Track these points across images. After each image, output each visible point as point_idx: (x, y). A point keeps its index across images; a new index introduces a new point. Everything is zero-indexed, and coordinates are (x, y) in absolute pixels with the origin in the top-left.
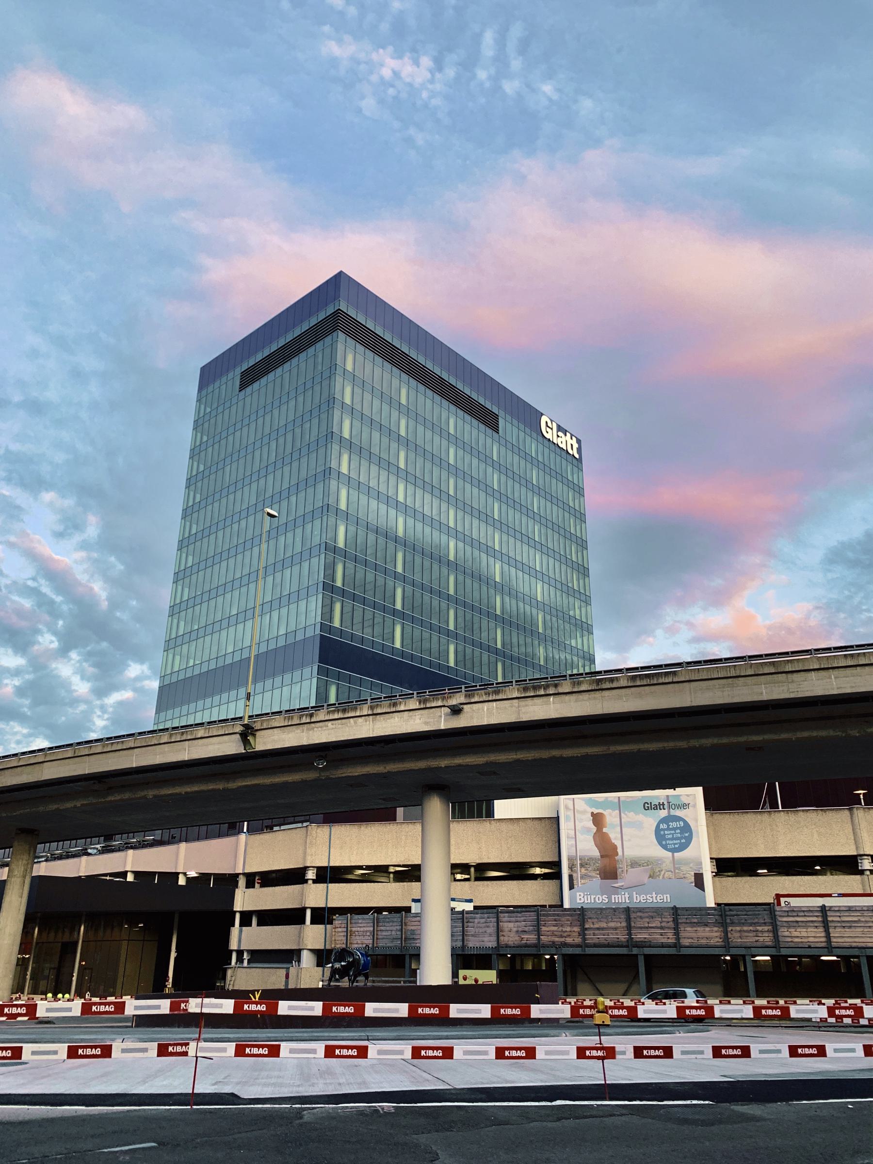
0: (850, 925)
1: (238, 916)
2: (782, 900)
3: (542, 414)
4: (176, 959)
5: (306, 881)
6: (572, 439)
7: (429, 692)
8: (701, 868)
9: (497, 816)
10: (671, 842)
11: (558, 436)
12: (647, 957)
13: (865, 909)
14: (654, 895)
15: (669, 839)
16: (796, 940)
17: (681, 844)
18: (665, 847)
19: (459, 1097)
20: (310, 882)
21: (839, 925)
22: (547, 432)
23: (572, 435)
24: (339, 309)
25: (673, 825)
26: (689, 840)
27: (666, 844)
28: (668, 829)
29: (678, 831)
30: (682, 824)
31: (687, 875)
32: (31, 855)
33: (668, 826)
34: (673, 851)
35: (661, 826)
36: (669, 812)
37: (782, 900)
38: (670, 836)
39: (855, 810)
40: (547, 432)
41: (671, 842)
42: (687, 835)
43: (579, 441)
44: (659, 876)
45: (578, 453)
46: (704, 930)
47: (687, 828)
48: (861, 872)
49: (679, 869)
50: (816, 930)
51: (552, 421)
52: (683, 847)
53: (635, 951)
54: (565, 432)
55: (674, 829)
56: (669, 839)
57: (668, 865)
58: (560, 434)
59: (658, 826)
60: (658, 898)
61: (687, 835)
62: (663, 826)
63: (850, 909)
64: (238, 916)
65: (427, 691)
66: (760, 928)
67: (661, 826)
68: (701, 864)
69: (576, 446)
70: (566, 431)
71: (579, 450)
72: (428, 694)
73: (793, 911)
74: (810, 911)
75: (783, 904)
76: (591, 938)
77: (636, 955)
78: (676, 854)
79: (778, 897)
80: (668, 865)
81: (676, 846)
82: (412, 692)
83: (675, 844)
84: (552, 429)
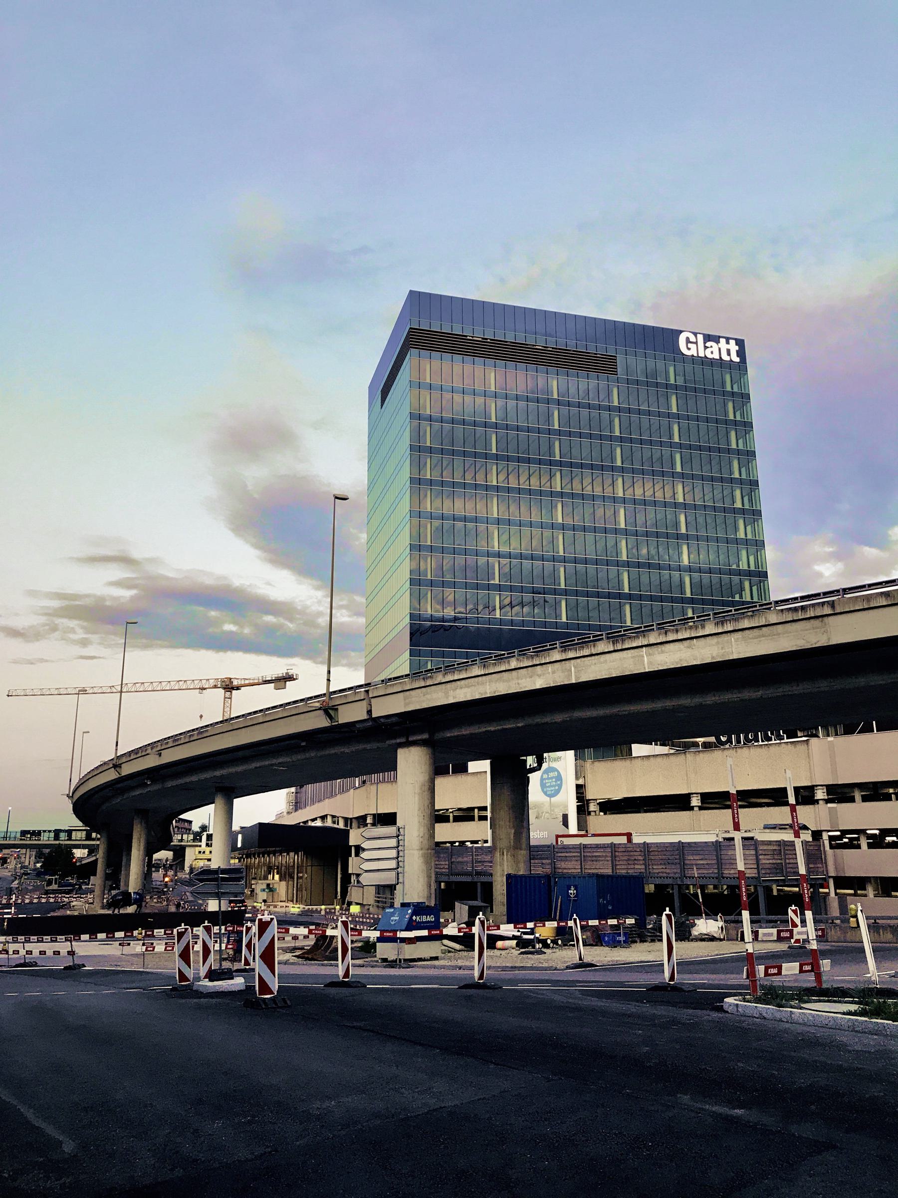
0: (596, 859)
1: (353, 849)
2: (560, 839)
3: (681, 332)
4: (341, 878)
5: (366, 825)
6: (728, 343)
7: (533, 649)
8: (567, 810)
9: (470, 771)
10: (549, 789)
11: (706, 348)
12: (483, 883)
13: (606, 846)
14: (538, 833)
15: (549, 787)
16: (565, 871)
17: (555, 789)
18: (545, 793)
19: (381, 981)
20: (369, 825)
21: (590, 859)
22: (689, 349)
23: (728, 340)
24: (411, 328)
25: (551, 775)
26: (560, 786)
27: (547, 791)
28: (548, 778)
29: (554, 780)
30: (556, 773)
31: (558, 816)
32: (143, 824)
33: (548, 775)
34: (550, 796)
35: (544, 777)
36: (549, 765)
37: (560, 839)
38: (549, 784)
39: (687, 753)
40: (689, 349)
41: (549, 789)
42: (559, 782)
43: (740, 343)
44: (541, 817)
45: (738, 356)
46: (582, 859)
47: (559, 778)
48: (692, 808)
49: (553, 811)
50: (576, 863)
51: (695, 334)
52: (557, 792)
53: (476, 879)
54: (716, 339)
55: (551, 778)
56: (549, 787)
57: (546, 808)
58: (708, 344)
59: (542, 776)
60: (541, 835)
61: (559, 782)
62: (545, 776)
63: (598, 846)
64: (353, 849)
65: (548, 644)
66: (544, 861)
67: (544, 777)
68: (566, 806)
69: (733, 347)
70: (719, 337)
71: (741, 353)
72: (532, 651)
73: (566, 848)
74: (574, 847)
75: (559, 843)
76: (459, 868)
77: (477, 882)
78: (552, 799)
79: (558, 836)
80: (546, 808)
81: (553, 792)
82: (503, 652)
83: (552, 790)
84: (696, 343)
